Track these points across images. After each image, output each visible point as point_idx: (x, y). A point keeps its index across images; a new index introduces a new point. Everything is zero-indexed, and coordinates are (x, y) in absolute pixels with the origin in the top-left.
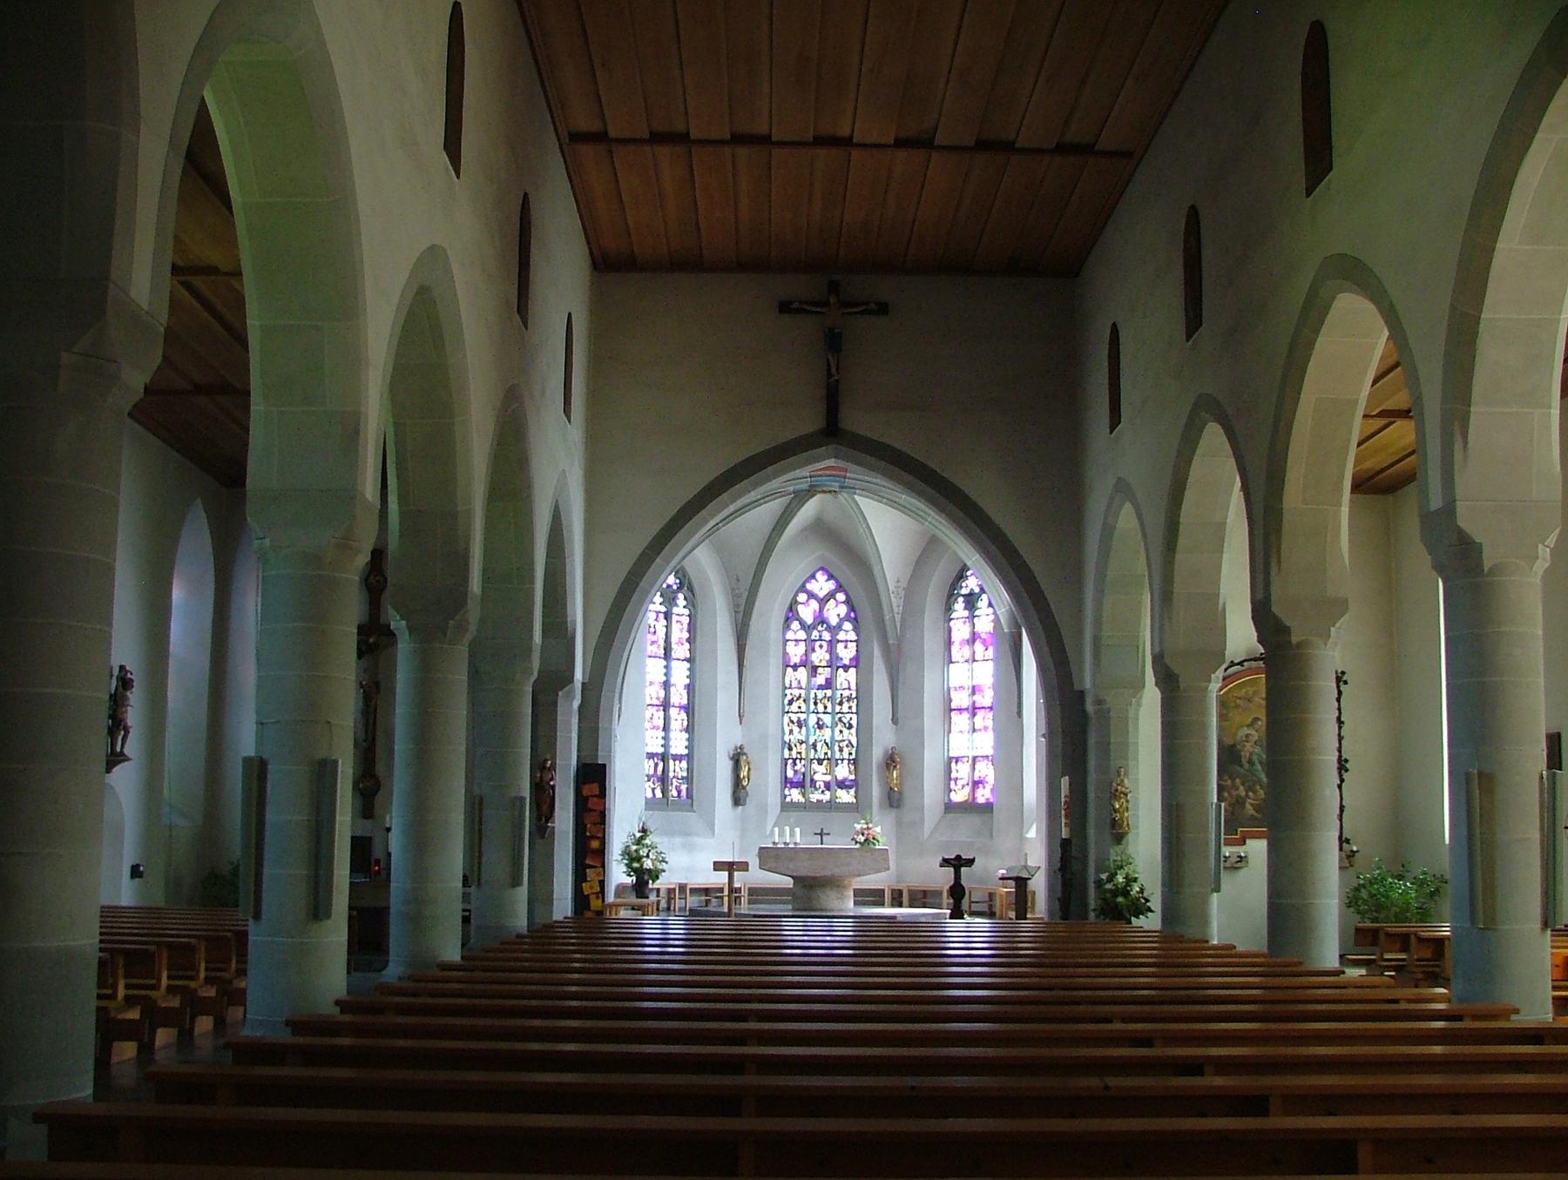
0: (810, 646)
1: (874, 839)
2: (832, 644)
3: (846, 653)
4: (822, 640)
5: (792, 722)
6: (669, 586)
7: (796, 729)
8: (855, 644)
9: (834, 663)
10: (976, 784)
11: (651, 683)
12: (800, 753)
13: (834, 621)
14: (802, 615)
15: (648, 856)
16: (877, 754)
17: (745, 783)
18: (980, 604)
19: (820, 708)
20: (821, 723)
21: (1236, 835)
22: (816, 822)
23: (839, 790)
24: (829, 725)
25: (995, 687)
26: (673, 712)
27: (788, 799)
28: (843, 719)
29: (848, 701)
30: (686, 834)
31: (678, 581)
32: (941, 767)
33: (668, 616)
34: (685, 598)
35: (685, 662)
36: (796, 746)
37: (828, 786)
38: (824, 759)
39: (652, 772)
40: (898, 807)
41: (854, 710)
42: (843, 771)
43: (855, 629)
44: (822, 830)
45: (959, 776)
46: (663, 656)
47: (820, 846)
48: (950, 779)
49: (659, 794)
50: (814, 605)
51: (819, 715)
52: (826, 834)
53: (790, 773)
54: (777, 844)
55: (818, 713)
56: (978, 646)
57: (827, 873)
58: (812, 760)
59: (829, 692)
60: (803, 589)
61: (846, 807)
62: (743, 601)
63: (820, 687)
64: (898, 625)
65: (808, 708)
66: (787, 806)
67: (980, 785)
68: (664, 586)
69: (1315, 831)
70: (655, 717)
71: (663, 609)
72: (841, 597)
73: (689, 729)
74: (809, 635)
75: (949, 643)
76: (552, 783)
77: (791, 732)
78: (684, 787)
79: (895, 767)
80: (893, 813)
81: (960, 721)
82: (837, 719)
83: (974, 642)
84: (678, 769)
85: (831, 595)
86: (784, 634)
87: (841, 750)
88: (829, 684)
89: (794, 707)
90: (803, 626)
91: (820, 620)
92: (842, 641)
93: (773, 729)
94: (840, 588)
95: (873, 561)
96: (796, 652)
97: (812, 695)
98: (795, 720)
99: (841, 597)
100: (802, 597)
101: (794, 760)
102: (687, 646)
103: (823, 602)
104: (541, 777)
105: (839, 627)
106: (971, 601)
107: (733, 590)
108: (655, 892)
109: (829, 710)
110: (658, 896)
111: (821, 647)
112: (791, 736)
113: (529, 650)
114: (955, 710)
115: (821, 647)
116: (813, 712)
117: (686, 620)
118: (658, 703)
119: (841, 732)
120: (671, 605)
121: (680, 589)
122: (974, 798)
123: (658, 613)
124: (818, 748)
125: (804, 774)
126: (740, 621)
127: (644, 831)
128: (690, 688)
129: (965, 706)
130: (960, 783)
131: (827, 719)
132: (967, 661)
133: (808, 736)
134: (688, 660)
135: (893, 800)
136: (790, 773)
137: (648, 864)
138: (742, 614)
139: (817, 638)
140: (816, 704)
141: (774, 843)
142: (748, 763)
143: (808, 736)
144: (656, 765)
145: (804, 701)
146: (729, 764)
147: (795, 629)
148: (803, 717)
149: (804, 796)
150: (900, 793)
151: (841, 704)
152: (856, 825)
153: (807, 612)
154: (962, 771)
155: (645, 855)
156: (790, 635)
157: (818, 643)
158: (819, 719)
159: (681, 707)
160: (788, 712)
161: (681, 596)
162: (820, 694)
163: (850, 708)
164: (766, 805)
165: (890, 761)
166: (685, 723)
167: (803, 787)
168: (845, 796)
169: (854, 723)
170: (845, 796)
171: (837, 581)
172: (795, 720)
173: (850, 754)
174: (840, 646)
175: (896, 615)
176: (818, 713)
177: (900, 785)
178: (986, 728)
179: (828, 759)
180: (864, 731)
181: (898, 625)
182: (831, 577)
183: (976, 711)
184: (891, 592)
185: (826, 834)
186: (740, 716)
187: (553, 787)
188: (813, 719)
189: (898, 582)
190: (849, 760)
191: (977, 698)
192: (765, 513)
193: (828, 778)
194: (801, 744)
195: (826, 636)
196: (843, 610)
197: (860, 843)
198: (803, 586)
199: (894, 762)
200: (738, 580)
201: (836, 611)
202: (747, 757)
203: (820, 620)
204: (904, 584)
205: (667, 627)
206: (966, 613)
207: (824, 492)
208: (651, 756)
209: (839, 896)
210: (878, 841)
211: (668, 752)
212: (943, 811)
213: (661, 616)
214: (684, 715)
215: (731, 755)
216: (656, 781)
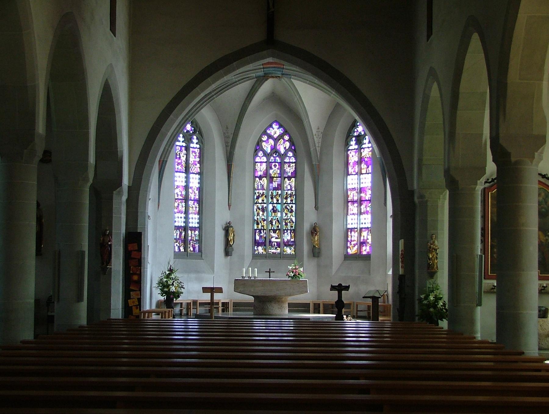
0: (269, 167)
1: (299, 274)
2: (282, 164)
3: (289, 170)
4: (276, 162)
5: (259, 209)
6: (188, 131)
7: (261, 213)
8: (294, 164)
9: (282, 175)
10: (362, 243)
11: (178, 187)
12: (263, 226)
13: (282, 151)
14: (265, 148)
15: (173, 284)
16: (307, 227)
17: (231, 244)
18: (365, 141)
19: (275, 201)
20: (275, 209)
21: (491, 273)
22: (269, 264)
23: (285, 247)
24: (280, 210)
25: (372, 189)
26: (191, 203)
27: (256, 252)
28: (288, 207)
29: (290, 197)
30: (197, 272)
31: (193, 129)
32: (342, 235)
33: (187, 148)
34: (197, 138)
35: (197, 175)
36: (261, 222)
37: (279, 245)
38: (277, 230)
39: (178, 237)
40: (318, 257)
41: (294, 202)
42: (287, 237)
43: (295, 156)
44: (270, 269)
45: (353, 239)
46: (184, 171)
47: (269, 279)
48: (347, 241)
49: (182, 249)
50: (271, 142)
51: (274, 205)
52: (272, 272)
53: (258, 238)
54: (245, 277)
55: (273, 203)
56: (363, 166)
57: (272, 294)
58: (270, 230)
59: (280, 192)
60: (265, 133)
61: (290, 257)
62: (230, 140)
63: (275, 189)
64: (319, 154)
65: (268, 200)
66: (256, 256)
67: (364, 245)
68: (185, 131)
69: (523, 270)
70: (180, 206)
71: (184, 144)
73: (200, 213)
74: (268, 159)
75: (347, 164)
76: (109, 243)
77: (258, 214)
78: (197, 246)
79: (316, 234)
80: (316, 260)
81: (354, 209)
82: (284, 207)
83: (361, 163)
84: (193, 235)
85: (281, 136)
86: (254, 159)
87: (286, 224)
88: (280, 187)
89: (260, 200)
90: (265, 154)
91: (275, 150)
92: (287, 163)
93: (248, 213)
94: (286, 132)
95: (303, 117)
96: (261, 168)
97: (270, 193)
98: (261, 207)
99: (287, 138)
100: (265, 138)
101: (260, 230)
102: (198, 165)
103: (276, 140)
104: (103, 240)
105: (285, 154)
106: (359, 140)
107: (224, 133)
108: (180, 305)
109: (280, 202)
110: (181, 307)
111: (275, 166)
112: (258, 217)
113: (85, 167)
114: (350, 201)
115: (275, 166)
116: (271, 203)
117: (197, 151)
118: (181, 198)
119: (286, 214)
120: (189, 142)
121: (194, 133)
122: (361, 252)
123: (181, 147)
124: (274, 223)
125: (265, 238)
126: (229, 152)
127: (171, 270)
128: (200, 189)
129: (356, 198)
130: (353, 243)
131: (279, 207)
132: (357, 174)
133: (267, 216)
134: (199, 174)
135: (315, 252)
136: (258, 238)
137: (173, 289)
138: (230, 147)
139: (273, 161)
140: (272, 198)
141: (243, 277)
142: (233, 232)
143: (267, 216)
144: (181, 233)
145: (265, 196)
146: (223, 233)
147: (261, 158)
148: (265, 205)
149: (265, 250)
150: (319, 249)
151: (286, 198)
152: (289, 267)
153: (267, 147)
154: (354, 236)
155: (171, 284)
156: (258, 159)
157: (273, 164)
158: (274, 207)
159: (195, 200)
160: (256, 203)
161: (195, 137)
162: (275, 193)
163: (292, 201)
164: (244, 256)
165: (314, 231)
166: (198, 209)
167: (265, 245)
168: (289, 251)
169: (294, 209)
170: (289, 251)
171: (284, 129)
172: (261, 207)
173: (292, 227)
174: (286, 166)
175: (317, 148)
176: (273, 203)
177: (320, 244)
178: (367, 212)
179: (279, 230)
180: (299, 213)
181: (319, 154)
182: (280, 126)
183: (362, 202)
184: (314, 134)
185: (272, 272)
186: (229, 205)
187: (110, 246)
188: (270, 207)
189: (318, 129)
190: (291, 230)
191: (363, 195)
192: (242, 88)
193: (279, 240)
194: (264, 221)
195: (278, 159)
196: (287, 144)
197: (291, 277)
198: (265, 133)
199: (316, 231)
200: (227, 128)
201: (283, 146)
202: (233, 229)
203: (275, 150)
204: (322, 130)
205: (186, 155)
206: (356, 147)
207: (273, 77)
208: (178, 228)
209: (279, 307)
210: (302, 276)
211: (188, 225)
212: (343, 259)
213: (183, 148)
214: (196, 205)
215: (224, 227)
216: (181, 242)
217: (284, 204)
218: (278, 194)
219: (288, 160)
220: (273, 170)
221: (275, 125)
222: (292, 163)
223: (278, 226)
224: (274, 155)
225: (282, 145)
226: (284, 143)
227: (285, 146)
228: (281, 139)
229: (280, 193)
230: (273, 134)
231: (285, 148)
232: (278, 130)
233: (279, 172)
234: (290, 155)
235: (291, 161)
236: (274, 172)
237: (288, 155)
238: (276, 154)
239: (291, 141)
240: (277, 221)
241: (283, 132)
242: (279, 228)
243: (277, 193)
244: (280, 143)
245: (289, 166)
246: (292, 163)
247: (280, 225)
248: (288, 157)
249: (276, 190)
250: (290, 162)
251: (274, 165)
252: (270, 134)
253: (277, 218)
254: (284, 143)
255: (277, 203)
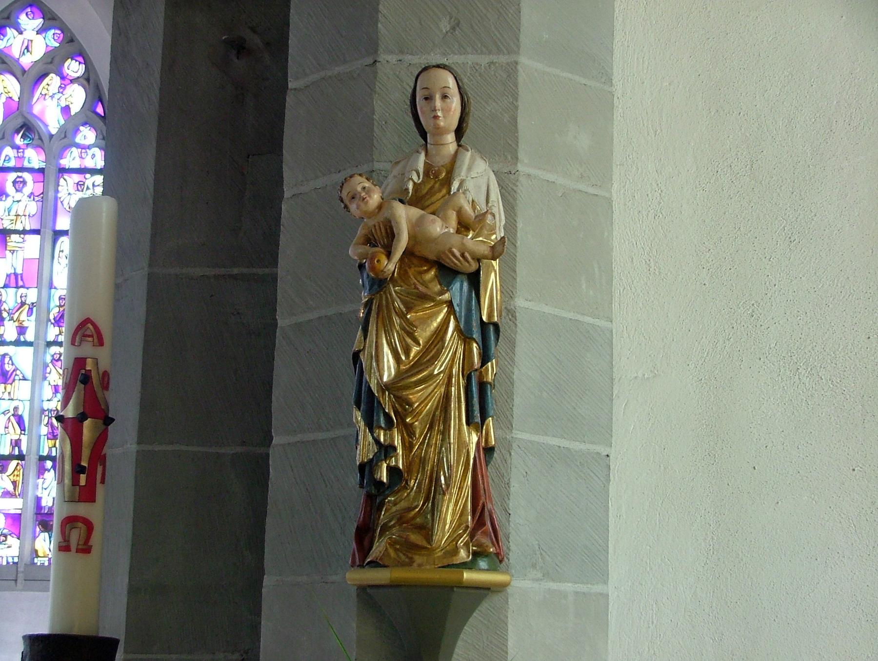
13: (53, 121)
24: (29, 374)
38: (11, 457)
58: (42, 459)
59: (32, 295)
72: (74, 68)
82: (48, 359)
109: (30, 336)
111: (19, 184)
139: (12, 164)
157: (12, 176)
171: (63, 29)
182: (51, 20)
196: (77, 97)
217: (49, 344)
218: (23, 304)
219: (78, 159)
220: (10, 199)
221: (27, 14)
222: (93, 172)
223: (17, 443)
224: (18, 140)
225: (52, 97)
226: (62, 88)
227: (63, 105)
228: (52, 75)
229: (34, 300)
230: (16, 52)
231: (66, 110)
232: (40, 37)
233: (33, 207)
234: (85, 137)
235: (89, 163)
236: (13, 213)
237: (79, 139)
238: (24, 137)
239: (88, 80)
240: (12, 418)
241: (57, 45)
242: (20, 451)
243: (19, 301)
244: (43, 93)
245: (79, 186)
246: (93, 172)
247: (24, 439)
248: (78, 146)
249: (17, 287)
250: (82, 171)
251: (15, 183)
252: (6, 51)
253: (16, 409)
254: (62, 88)
255: (17, 343)
